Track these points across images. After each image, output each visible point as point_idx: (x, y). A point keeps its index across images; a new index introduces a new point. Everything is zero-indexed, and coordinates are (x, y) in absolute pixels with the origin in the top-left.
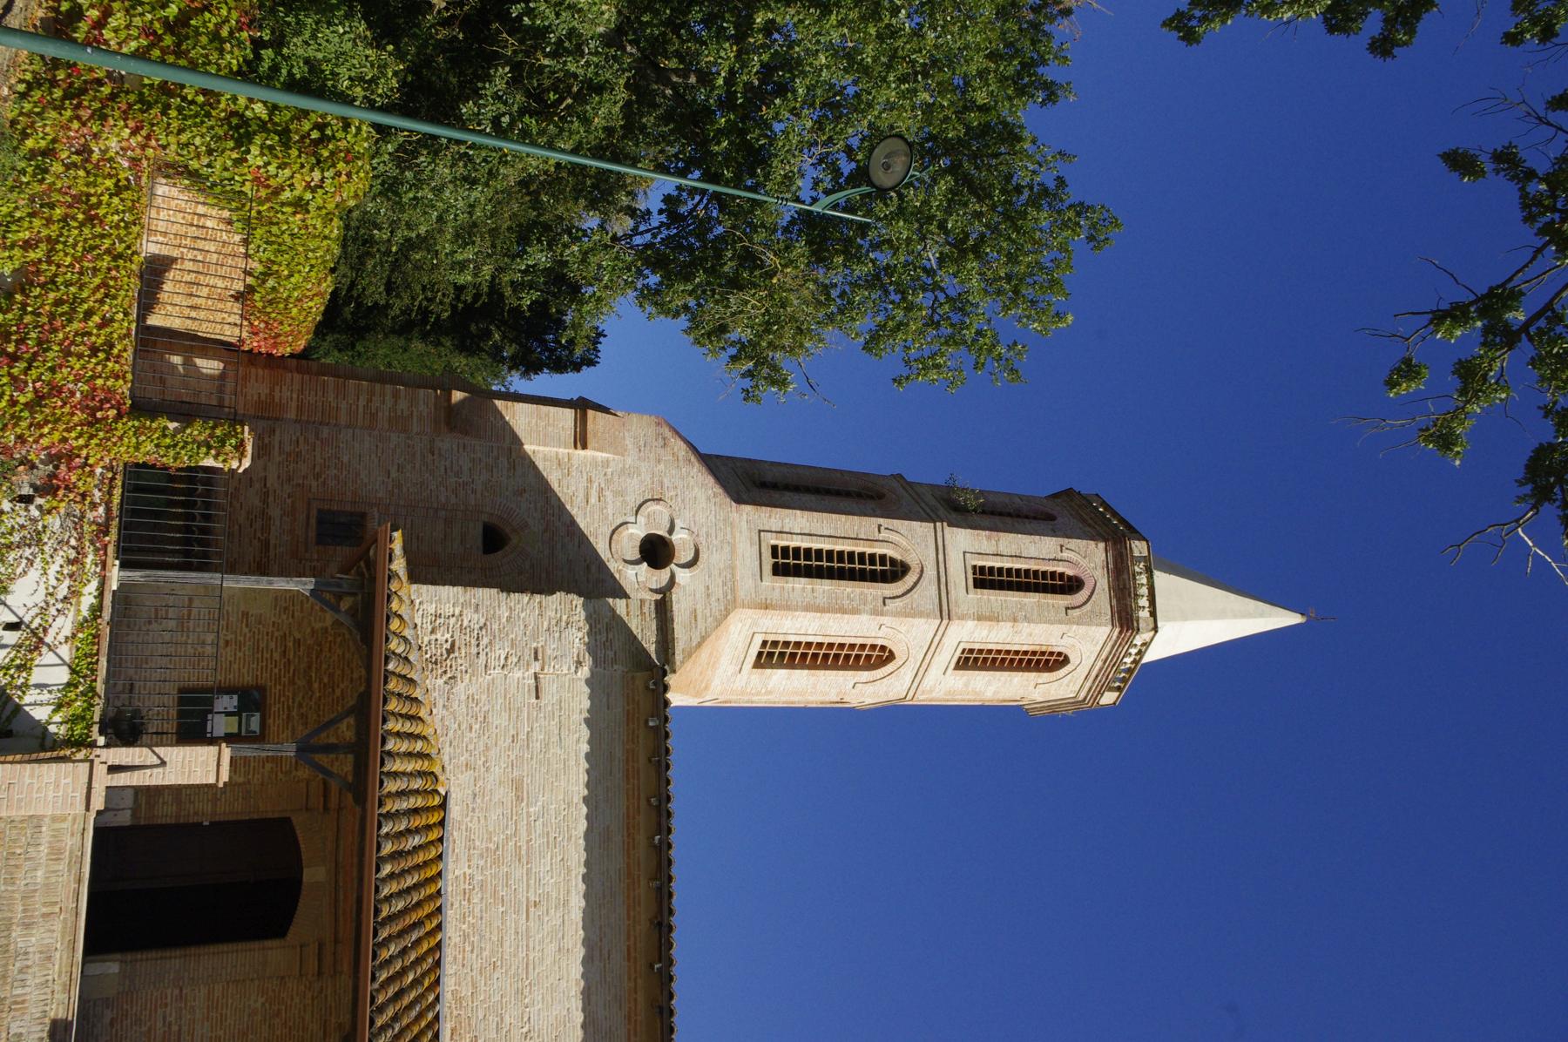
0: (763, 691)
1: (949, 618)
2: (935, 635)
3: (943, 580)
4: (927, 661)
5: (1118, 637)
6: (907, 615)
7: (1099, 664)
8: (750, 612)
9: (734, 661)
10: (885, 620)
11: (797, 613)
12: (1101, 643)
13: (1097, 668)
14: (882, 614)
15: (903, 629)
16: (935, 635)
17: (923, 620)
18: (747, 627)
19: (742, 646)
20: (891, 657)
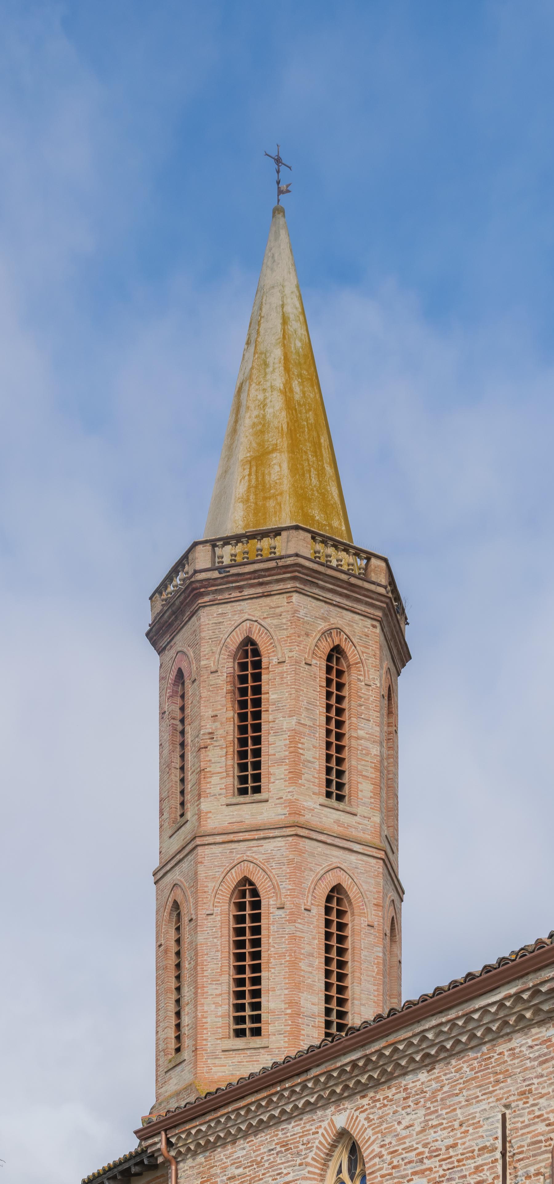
0: (289, 1011)
1: (195, 838)
2: (215, 844)
3: (179, 857)
4: (247, 836)
5: (208, 593)
6: (196, 892)
7: (247, 592)
8: (200, 1064)
9: (254, 1058)
10: (202, 913)
11: (199, 1014)
12: (221, 609)
13: (252, 591)
14: (197, 919)
15: (211, 885)
16: (215, 844)
17: (201, 868)
18: (217, 1061)
19: (237, 1058)
20: (246, 881)
